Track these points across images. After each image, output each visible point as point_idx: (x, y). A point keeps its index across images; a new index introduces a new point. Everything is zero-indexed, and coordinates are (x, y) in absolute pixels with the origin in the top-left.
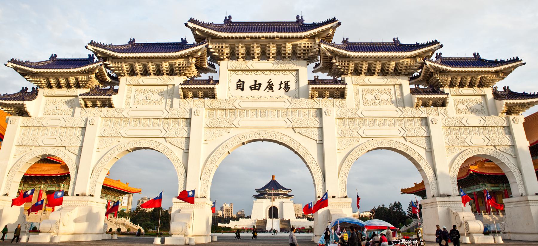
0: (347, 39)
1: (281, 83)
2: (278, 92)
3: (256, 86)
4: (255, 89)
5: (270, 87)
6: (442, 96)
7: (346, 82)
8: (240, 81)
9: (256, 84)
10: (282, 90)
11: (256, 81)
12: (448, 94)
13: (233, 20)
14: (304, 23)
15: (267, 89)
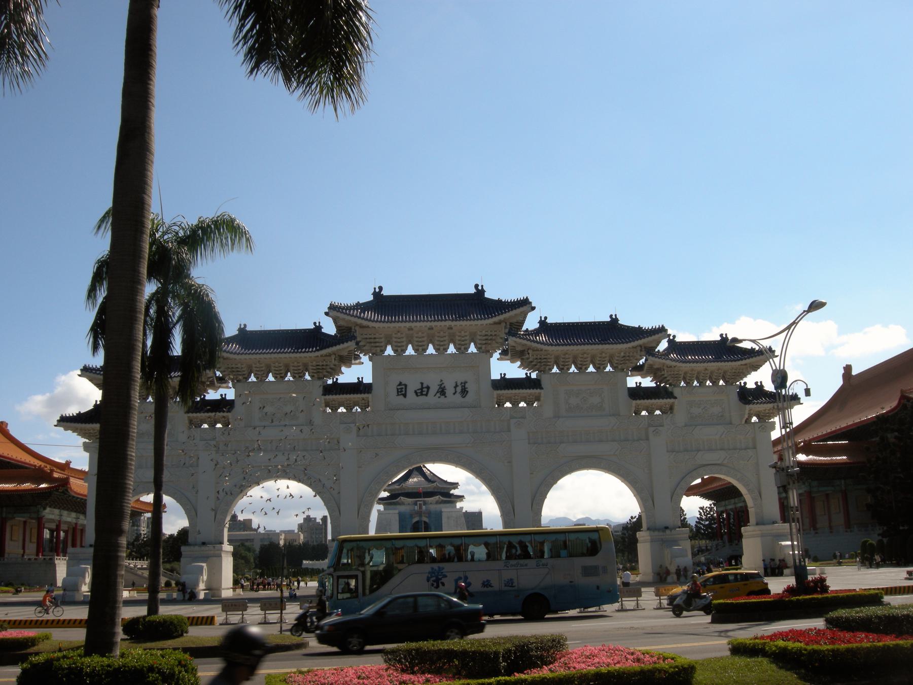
0: (546, 318)
1: (456, 386)
2: (452, 398)
3: (423, 391)
4: (422, 395)
5: (442, 391)
6: (669, 400)
7: (544, 383)
8: (400, 384)
9: (422, 388)
10: (458, 395)
11: (422, 384)
12: (675, 398)
13: (385, 293)
14: (487, 295)
15: (438, 395)
